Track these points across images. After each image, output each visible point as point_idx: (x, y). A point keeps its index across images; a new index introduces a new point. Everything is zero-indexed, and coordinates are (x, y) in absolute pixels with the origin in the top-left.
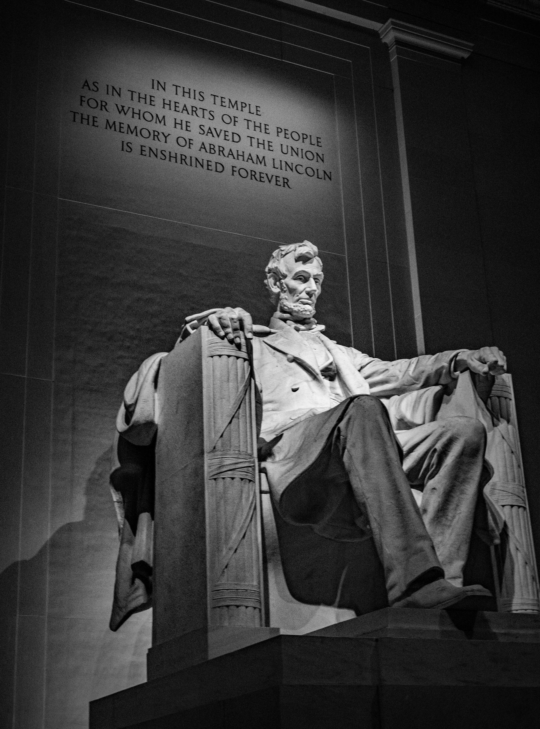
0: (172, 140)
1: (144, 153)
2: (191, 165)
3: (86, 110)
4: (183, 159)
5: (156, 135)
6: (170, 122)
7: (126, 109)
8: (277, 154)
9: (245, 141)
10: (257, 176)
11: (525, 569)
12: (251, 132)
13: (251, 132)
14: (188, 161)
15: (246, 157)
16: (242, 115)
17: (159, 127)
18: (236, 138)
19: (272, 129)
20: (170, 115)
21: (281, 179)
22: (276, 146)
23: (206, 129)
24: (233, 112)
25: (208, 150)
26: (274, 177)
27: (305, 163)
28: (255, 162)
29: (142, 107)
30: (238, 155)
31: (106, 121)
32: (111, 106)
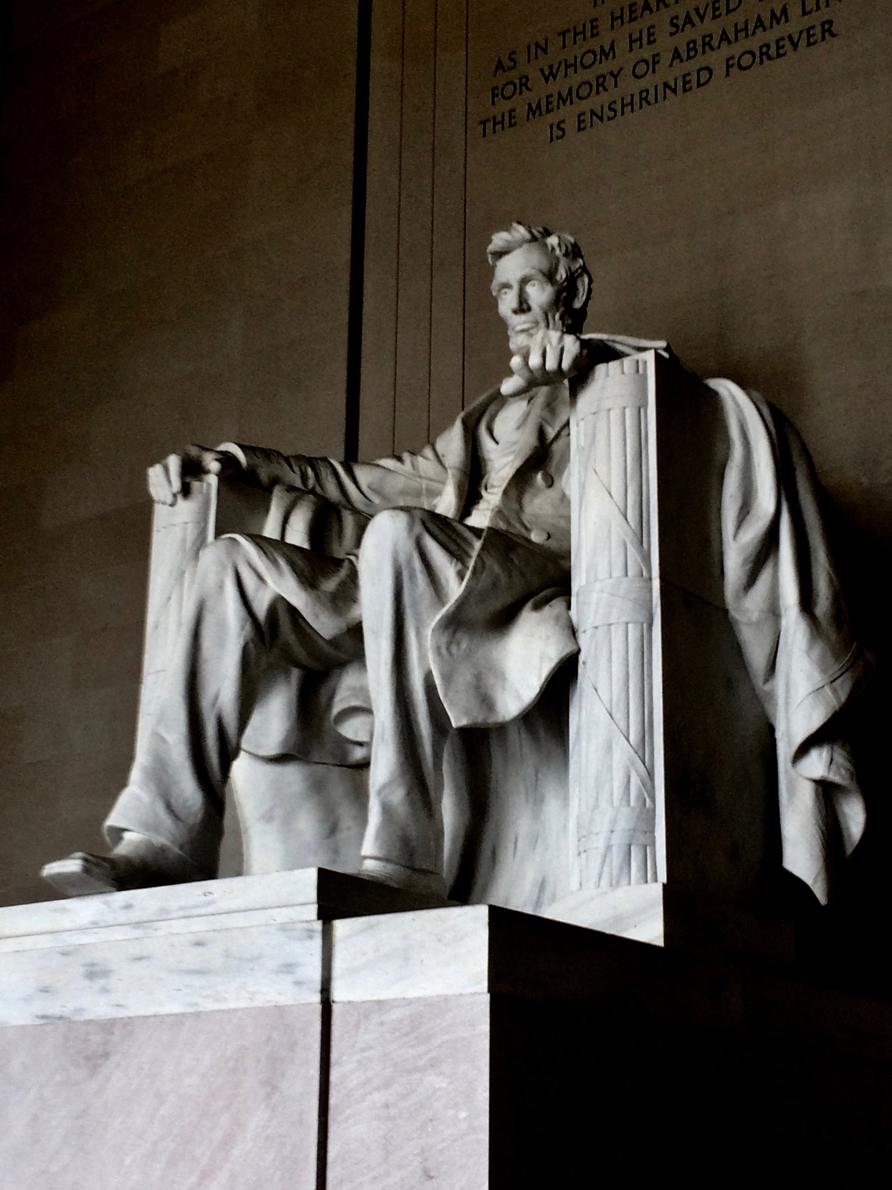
1: (582, 126)
2: (656, 101)
5: (601, 83)
6: (622, 45)
7: (554, 71)
10: (773, 52)
11: (609, 749)
14: (651, 98)
15: (751, 27)
17: (605, 67)
21: (818, 29)
23: (681, 23)
25: (684, 57)
26: (805, 34)
28: (767, 23)
30: (737, 32)
31: (527, 107)
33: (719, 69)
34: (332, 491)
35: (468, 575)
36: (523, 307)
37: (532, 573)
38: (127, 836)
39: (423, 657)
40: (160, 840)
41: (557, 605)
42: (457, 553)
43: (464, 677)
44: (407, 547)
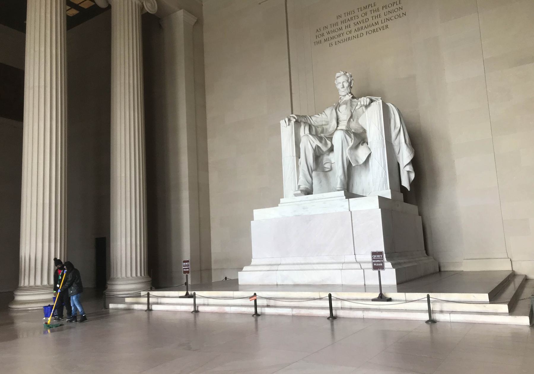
0: (345, 35)
3: (318, 39)
4: (349, 39)
5: (339, 35)
6: (344, 28)
8: (383, 17)
9: (370, 19)
12: (373, 14)
13: (373, 14)
16: (368, 10)
18: (367, 20)
19: (381, 9)
20: (343, 26)
22: (382, 15)
24: (364, 11)
27: (395, 14)
29: (335, 28)
32: (325, 34)
33: (365, 33)
34: (309, 122)
35: (353, 140)
36: (343, 87)
37: (361, 138)
38: (301, 187)
39: (346, 154)
40: (307, 187)
41: (365, 144)
42: (350, 137)
43: (353, 158)
44: (343, 136)
